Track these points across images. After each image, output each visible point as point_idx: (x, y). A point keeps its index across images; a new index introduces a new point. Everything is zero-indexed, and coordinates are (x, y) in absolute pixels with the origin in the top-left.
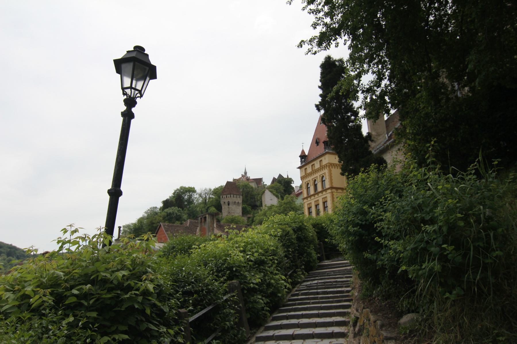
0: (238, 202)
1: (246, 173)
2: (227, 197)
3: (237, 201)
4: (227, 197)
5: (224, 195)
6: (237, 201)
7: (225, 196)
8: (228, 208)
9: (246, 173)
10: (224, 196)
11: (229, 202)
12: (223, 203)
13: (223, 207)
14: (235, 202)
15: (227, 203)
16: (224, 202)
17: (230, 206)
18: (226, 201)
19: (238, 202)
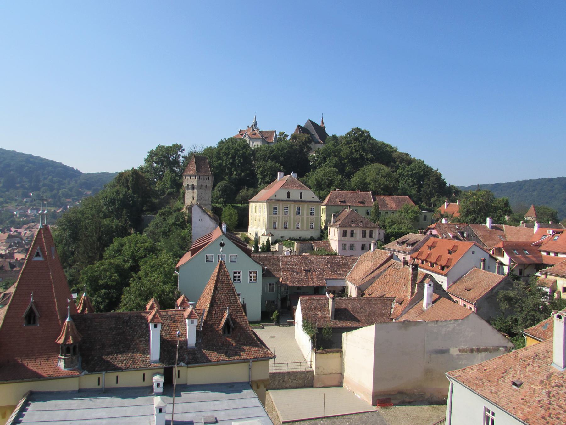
0: (206, 185)
1: (256, 122)
2: (191, 179)
3: (204, 185)
4: (191, 179)
5: (188, 175)
6: (204, 185)
7: (189, 178)
8: (193, 193)
9: (256, 122)
10: (187, 177)
11: (193, 185)
12: (186, 185)
13: (187, 191)
14: (202, 185)
15: (190, 187)
16: (188, 185)
17: (196, 191)
18: (190, 184)
19: (206, 185)
